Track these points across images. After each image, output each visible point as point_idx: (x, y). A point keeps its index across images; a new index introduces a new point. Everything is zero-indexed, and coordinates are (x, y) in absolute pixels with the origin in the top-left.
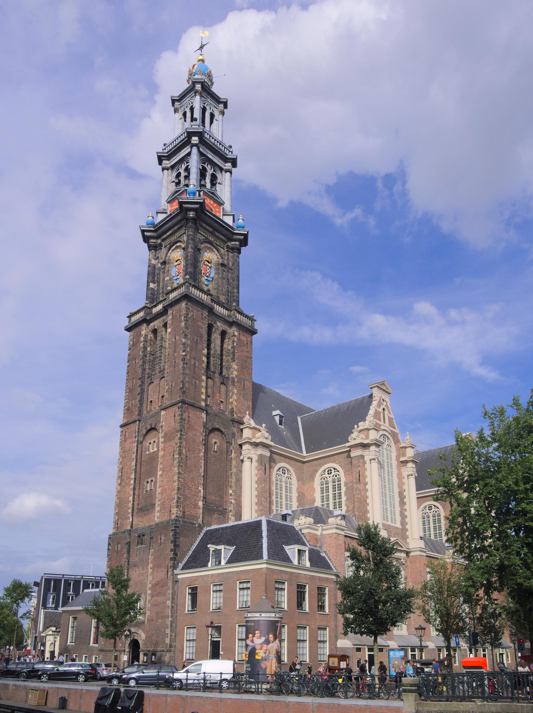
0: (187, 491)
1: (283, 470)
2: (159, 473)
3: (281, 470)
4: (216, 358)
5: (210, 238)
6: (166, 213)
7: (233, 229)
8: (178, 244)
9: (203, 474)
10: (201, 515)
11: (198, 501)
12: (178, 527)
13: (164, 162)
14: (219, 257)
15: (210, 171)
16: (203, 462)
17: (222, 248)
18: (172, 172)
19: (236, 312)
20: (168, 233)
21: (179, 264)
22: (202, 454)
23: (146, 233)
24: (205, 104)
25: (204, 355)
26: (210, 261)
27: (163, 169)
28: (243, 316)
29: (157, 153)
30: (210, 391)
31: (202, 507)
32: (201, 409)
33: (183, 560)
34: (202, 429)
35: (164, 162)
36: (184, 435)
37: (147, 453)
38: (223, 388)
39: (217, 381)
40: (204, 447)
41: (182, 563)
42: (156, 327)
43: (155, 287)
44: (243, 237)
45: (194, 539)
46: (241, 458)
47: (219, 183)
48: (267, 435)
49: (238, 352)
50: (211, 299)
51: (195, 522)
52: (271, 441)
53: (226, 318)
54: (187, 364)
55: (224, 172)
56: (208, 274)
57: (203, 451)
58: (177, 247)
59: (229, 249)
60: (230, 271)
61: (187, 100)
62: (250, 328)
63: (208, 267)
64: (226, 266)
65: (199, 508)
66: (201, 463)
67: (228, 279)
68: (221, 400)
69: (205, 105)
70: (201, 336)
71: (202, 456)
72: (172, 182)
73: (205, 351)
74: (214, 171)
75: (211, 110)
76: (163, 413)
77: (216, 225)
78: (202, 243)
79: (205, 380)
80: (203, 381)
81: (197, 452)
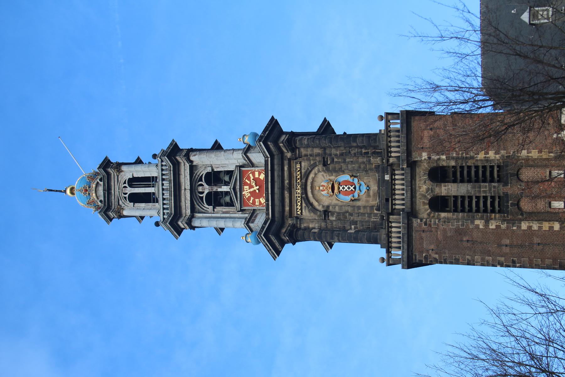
4: (480, 192)
5: (299, 191)
7: (268, 160)
14: (316, 168)
15: (206, 189)
17: (301, 166)
24: (125, 198)
26: (330, 186)
38: (527, 174)
44: (269, 143)
47: (213, 170)
55: (194, 164)
59: (295, 154)
60: (328, 151)
63: (341, 188)
64: (324, 158)
67: (342, 154)
69: (127, 196)
74: (201, 180)
75: (125, 185)
77: (276, 190)
78: (311, 204)
80: (530, 227)
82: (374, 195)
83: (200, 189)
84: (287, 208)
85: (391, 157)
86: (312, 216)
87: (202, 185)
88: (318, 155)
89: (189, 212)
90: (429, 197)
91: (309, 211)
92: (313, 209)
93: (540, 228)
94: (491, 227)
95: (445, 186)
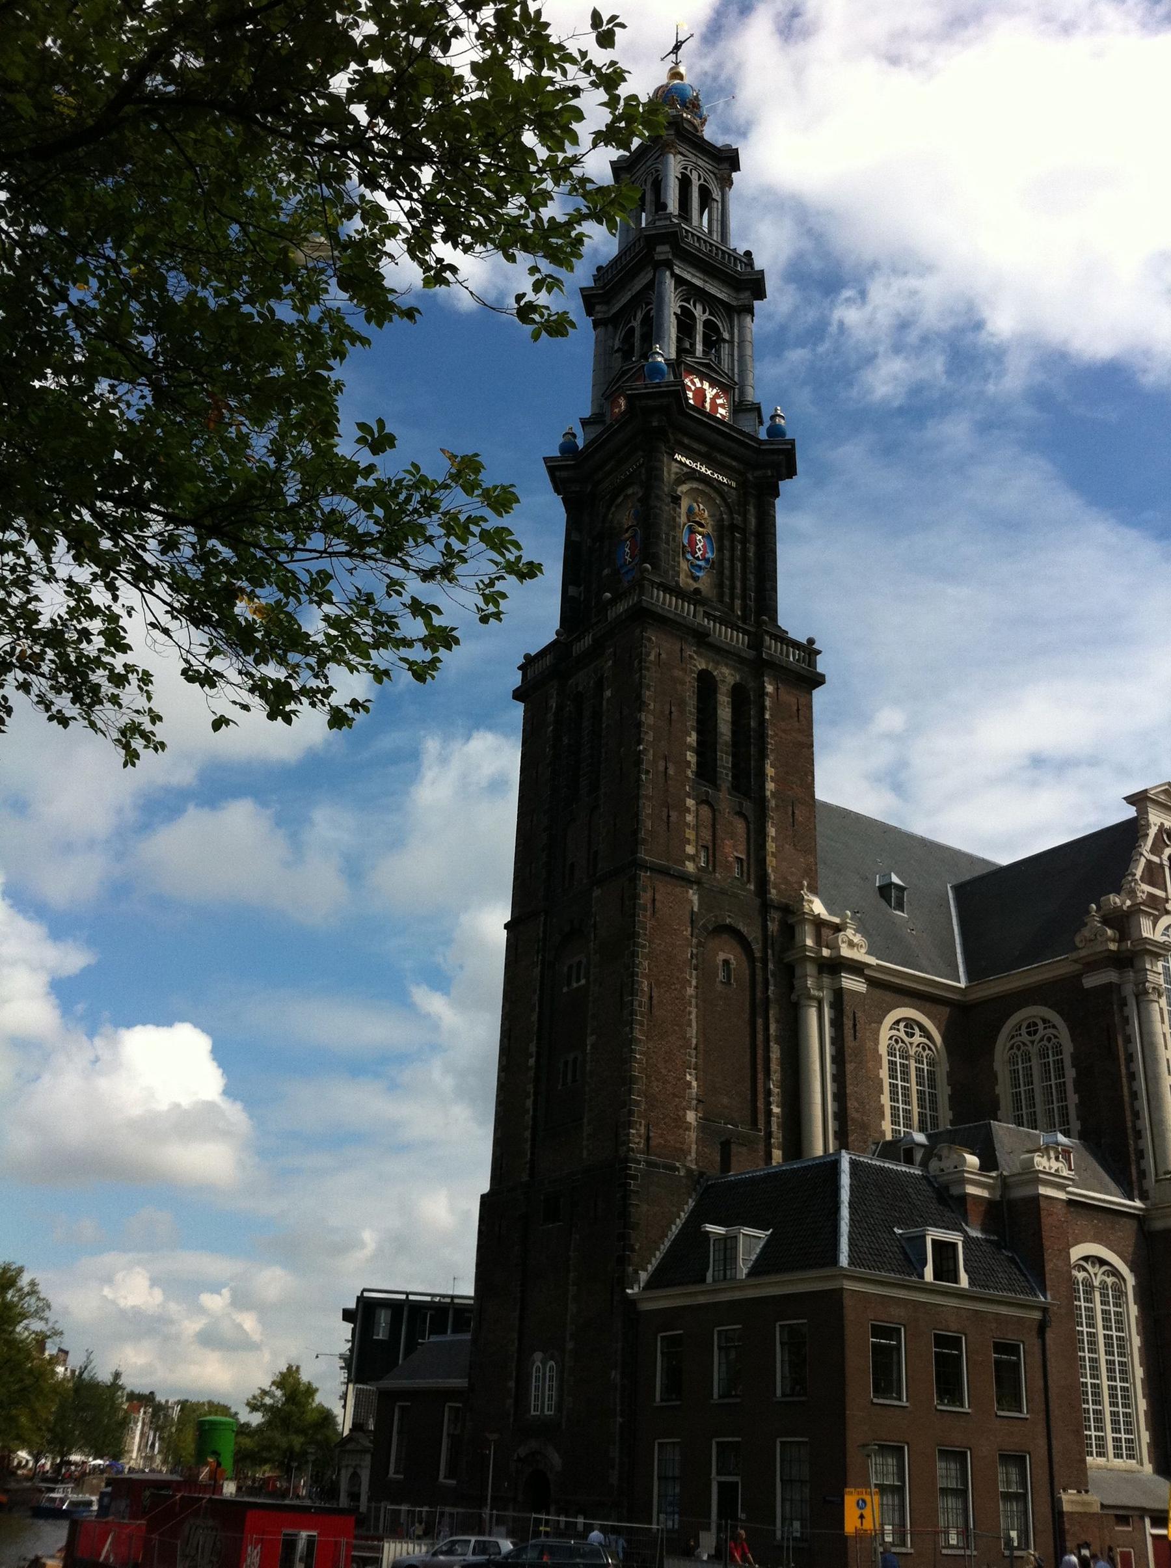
0: (655, 1084)
1: (906, 1026)
2: (590, 1040)
3: (902, 1025)
4: (722, 752)
5: (703, 470)
6: (603, 422)
8: (630, 491)
9: (694, 1041)
10: (694, 1147)
11: (684, 1109)
12: (634, 1178)
13: (598, 308)
15: (700, 314)
16: (694, 1011)
18: (616, 328)
19: (767, 638)
20: (607, 468)
21: (633, 537)
22: (690, 991)
23: (558, 474)
24: (685, 168)
25: (690, 748)
27: (596, 324)
28: (787, 646)
29: (582, 289)
30: (706, 835)
31: (694, 1123)
32: (686, 880)
33: (650, 1262)
34: (689, 929)
35: (598, 308)
36: (644, 946)
37: (565, 990)
39: (724, 809)
40: (694, 972)
41: (646, 1270)
42: (580, 688)
43: (580, 594)
45: (675, 1209)
46: (794, 997)
48: (857, 939)
49: (776, 735)
50: (705, 612)
51: (678, 1164)
52: (868, 953)
53: (744, 655)
54: (647, 772)
56: (699, 554)
57: (694, 983)
58: (627, 497)
61: (649, 163)
62: (805, 673)
65: (688, 1129)
66: (690, 1013)
68: (736, 854)
69: (689, 173)
70: (682, 703)
71: (691, 996)
72: (616, 351)
73: (692, 739)
76: (597, 892)
78: (684, 483)
79: (693, 808)
80: (688, 810)
81: (678, 986)
82: (688, 584)
83: (699, 307)
84: (686, 441)
85: (771, 639)
86: (673, 476)
87: (704, 312)
88: (745, 520)
89: (677, 271)
90: (715, 673)
91: (677, 473)
92: (680, 481)
93: (688, 825)
94: (688, 753)
95: (728, 703)
